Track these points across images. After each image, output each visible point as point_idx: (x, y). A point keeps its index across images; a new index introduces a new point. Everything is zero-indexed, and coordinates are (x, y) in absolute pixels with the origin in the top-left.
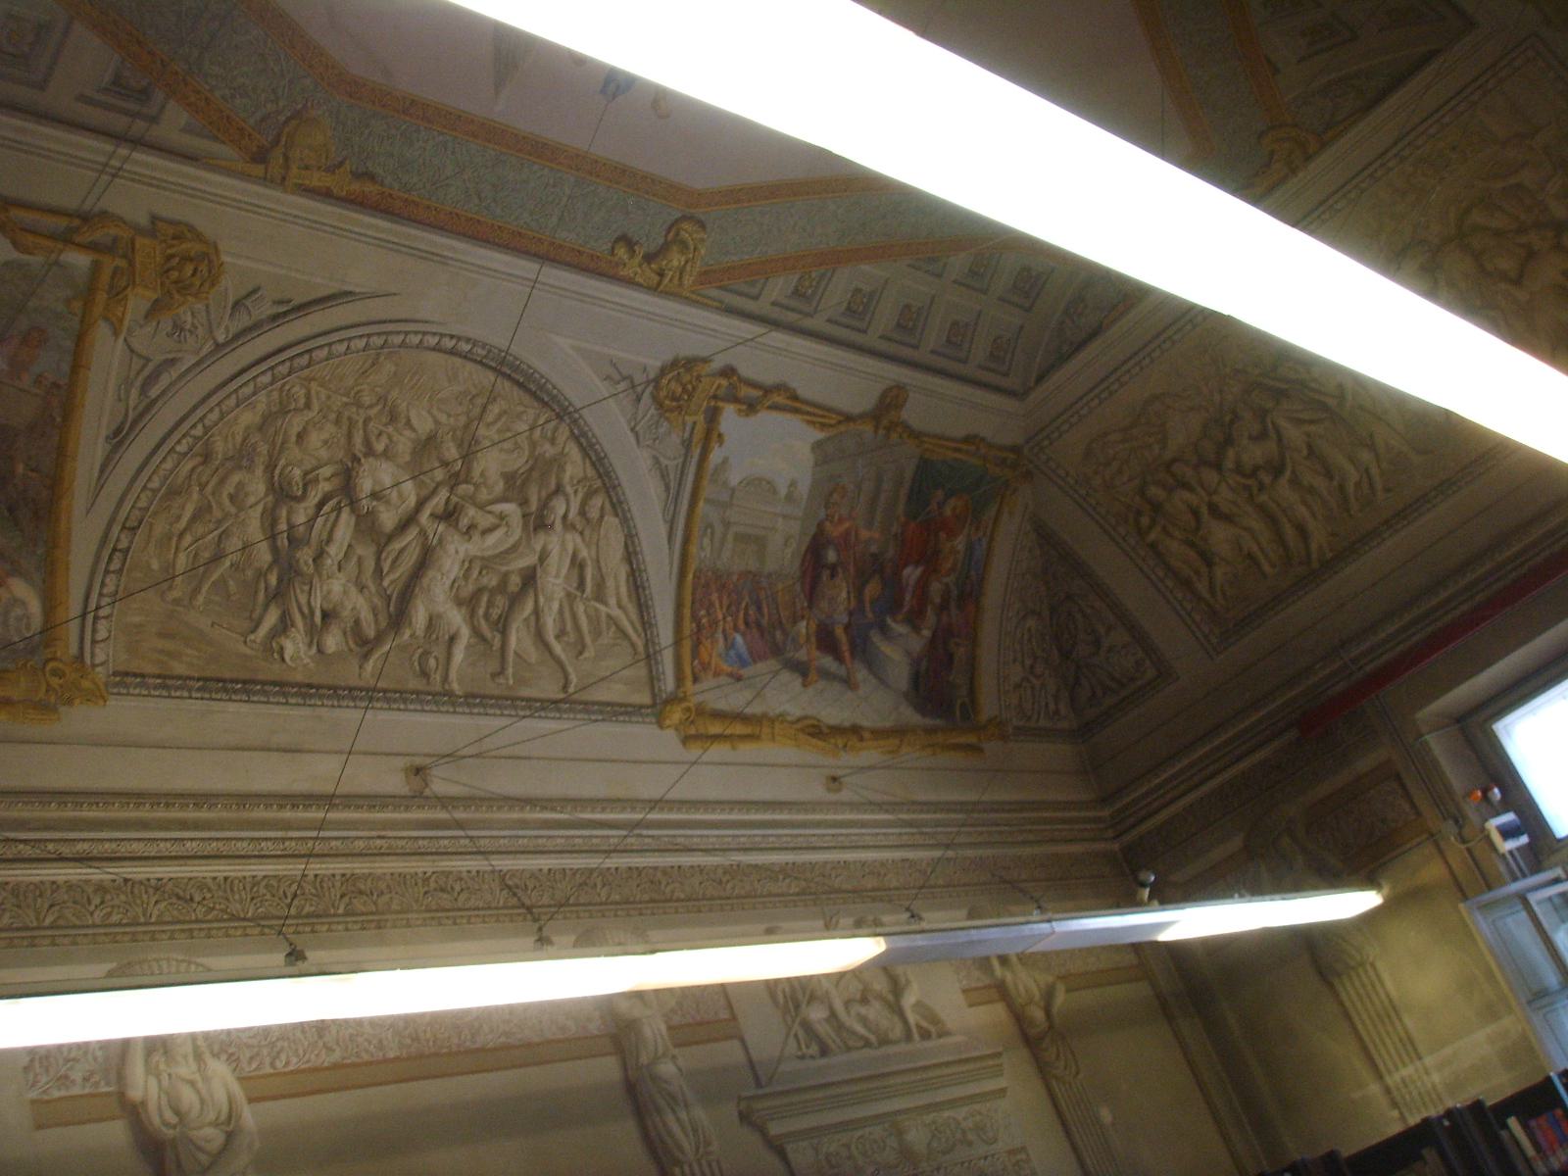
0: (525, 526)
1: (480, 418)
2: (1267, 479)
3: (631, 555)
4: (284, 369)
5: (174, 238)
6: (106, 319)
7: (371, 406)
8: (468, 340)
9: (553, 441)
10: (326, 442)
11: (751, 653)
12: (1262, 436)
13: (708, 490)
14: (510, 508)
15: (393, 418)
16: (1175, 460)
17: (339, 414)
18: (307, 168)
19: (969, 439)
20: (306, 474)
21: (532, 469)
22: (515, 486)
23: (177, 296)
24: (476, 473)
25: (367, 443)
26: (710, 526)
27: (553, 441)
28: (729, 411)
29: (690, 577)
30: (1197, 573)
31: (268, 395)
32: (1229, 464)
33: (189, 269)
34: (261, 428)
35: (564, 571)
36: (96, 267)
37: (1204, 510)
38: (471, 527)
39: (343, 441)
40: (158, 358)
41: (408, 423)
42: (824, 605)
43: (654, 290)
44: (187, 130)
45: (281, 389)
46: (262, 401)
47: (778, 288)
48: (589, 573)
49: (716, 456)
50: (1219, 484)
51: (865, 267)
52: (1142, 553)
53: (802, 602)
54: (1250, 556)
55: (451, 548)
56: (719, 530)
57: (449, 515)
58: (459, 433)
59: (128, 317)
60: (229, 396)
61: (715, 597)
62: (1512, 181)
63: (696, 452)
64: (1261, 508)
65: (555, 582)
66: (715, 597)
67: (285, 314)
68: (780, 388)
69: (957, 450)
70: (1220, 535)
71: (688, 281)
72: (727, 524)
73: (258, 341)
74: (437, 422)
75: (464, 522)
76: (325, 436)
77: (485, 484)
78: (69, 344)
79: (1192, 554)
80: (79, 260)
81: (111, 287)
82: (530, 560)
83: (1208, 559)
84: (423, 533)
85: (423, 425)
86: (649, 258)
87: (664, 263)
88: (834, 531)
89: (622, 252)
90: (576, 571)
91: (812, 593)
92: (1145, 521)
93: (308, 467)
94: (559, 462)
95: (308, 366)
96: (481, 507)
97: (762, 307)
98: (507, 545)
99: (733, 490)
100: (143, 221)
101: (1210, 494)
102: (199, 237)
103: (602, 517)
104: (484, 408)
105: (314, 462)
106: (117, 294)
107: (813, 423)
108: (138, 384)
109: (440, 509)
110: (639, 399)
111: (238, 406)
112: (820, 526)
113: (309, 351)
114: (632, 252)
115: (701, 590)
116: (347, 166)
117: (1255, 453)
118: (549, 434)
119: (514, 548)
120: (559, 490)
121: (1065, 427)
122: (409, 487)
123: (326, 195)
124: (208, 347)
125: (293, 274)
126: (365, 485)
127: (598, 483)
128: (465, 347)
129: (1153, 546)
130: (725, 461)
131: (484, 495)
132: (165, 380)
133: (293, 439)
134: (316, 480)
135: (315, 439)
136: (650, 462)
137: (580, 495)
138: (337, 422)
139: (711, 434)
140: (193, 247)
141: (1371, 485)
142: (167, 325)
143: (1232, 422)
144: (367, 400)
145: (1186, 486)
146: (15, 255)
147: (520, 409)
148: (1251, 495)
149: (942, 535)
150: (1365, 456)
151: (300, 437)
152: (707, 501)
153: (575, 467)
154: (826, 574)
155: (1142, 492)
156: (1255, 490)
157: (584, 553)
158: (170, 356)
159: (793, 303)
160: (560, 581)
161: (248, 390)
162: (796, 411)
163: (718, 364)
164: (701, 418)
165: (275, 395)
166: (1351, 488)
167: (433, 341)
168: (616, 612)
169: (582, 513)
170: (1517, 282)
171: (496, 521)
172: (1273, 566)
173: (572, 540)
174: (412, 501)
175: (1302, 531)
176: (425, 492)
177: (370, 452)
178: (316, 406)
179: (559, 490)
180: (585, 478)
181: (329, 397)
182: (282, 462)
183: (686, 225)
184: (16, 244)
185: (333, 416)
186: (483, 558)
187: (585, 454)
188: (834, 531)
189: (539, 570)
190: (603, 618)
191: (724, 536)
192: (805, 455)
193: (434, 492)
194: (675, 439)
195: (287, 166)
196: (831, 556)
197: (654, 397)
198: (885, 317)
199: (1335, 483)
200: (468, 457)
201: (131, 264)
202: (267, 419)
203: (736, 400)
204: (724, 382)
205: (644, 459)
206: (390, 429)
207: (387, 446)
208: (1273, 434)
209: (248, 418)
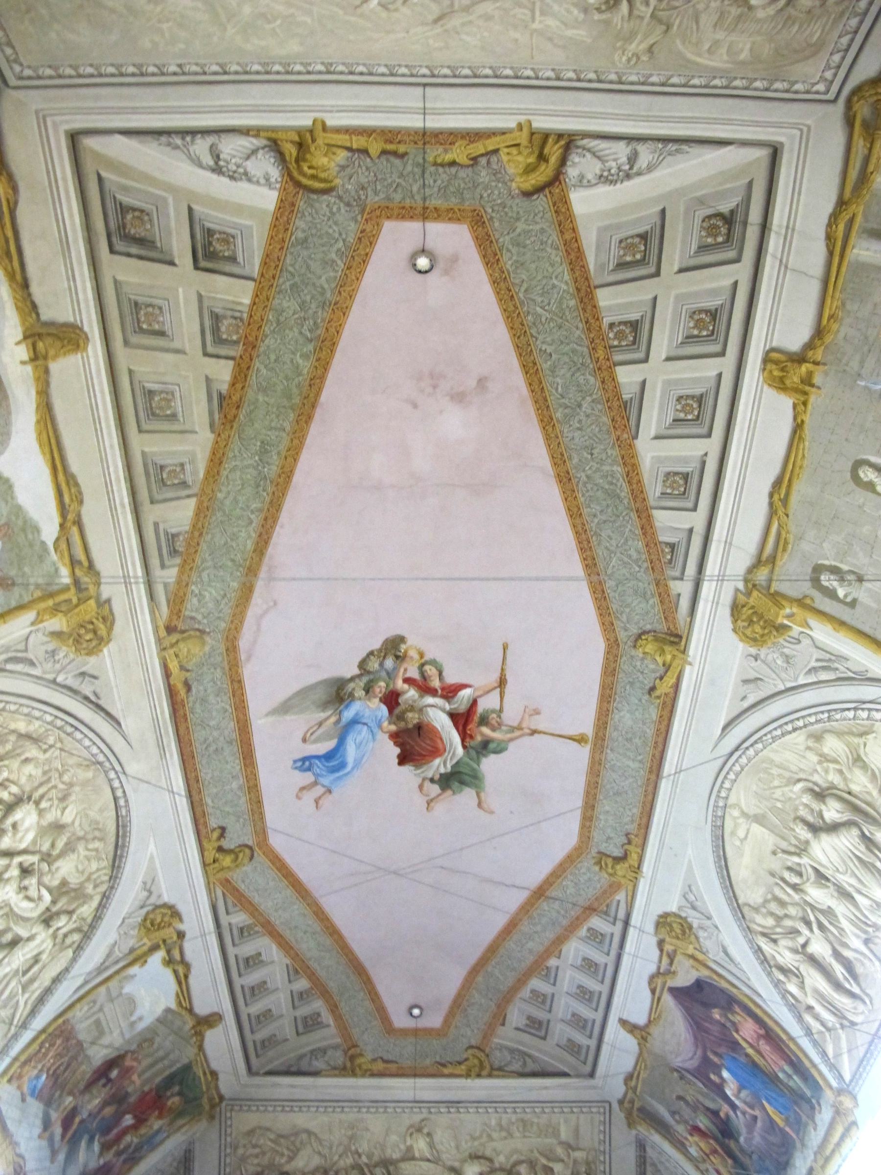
0: (43, 913)
1: (87, 841)
3: (57, 980)
4: (59, 723)
5: (103, 618)
6: (38, 614)
7: (63, 783)
8: (127, 801)
9: (96, 886)
10: (30, 775)
11: (41, 1090)
13: (113, 984)
14: (47, 897)
15: (63, 798)
17: (50, 770)
18: (177, 656)
19: (214, 1074)
20: (7, 780)
21: (75, 890)
22: (62, 890)
23: (71, 641)
24: (57, 864)
25: (42, 797)
26: (95, 1002)
27: (96, 886)
28: (161, 954)
29: (60, 1021)
31: (40, 727)
33: (88, 637)
34: (21, 736)
35: (29, 956)
36: (66, 589)
38: (26, 888)
39: (36, 784)
40: (30, 655)
41: (64, 809)
42: (87, 1097)
43: (205, 865)
44: (166, 585)
45: (47, 730)
46: (35, 727)
47: (240, 918)
48: (36, 969)
49: (135, 970)
51: (274, 947)
53: (81, 1086)
55: (8, 888)
56: (95, 1009)
57: (25, 871)
58: (73, 838)
59: (45, 624)
60: (28, 706)
61: (59, 1042)
62: (551, 1165)
63: (131, 958)
65: (20, 957)
66: (59, 1042)
67: (91, 702)
68: (187, 966)
69: (205, 1074)
71: (219, 875)
72: (101, 1009)
73: (67, 698)
74: (73, 822)
75: (26, 882)
76: (34, 773)
77: (53, 874)
78: (13, 604)
80: (65, 577)
81: (59, 604)
82: (23, 933)
84: (8, 867)
85: (67, 818)
86: (220, 849)
87: (221, 857)
88: (128, 1062)
89: (216, 835)
90: (32, 961)
91: (90, 1085)
93: (11, 777)
94: (87, 898)
95: (68, 734)
96: (40, 883)
97: (224, 919)
98: (26, 915)
99: (120, 994)
100: (104, 596)
102: (110, 629)
103: (70, 946)
104: (94, 839)
105: (16, 779)
106: (55, 610)
107: (177, 995)
108: (10, 655)
109: (26, 865)
110: (142, 907)
111: (26, 715)
112: (127, 1052)
113: (76, 729)
114: (219, 839)
115: (61, 1033)
116: (188, 674)
118: (98, 881)
119: (26, 920)
120: (70, 913)
122: (30, 836)
123: (167, 674)
124: (50, 677)
125: (115, 690)
126: (18, 815)
127: (85, 928)
128: (122, 802)
130: (133, 977)
131: (46, 879)
132: (19, 667)
133: (23, 757)
134: (6, 788)
135: (29, 769)
136: (112, 941)
137: (75, 926)
138: (45, 773)
139: (138, 958)
140: (102, 631)
142: (50, 647)
144: (66, 778)
146: (50, 544)
147: (104, 857)
149: (157, 1113)
151: (27, 760)
152: (108, 990)
153: (87, 910)
154: (103, 1081)
157: (44, 957)
158: (35, 661)
159: (235, 932)
160: (22, 959)
161: (37, 714)
162: (179, 983)
163: (181, 927)
164: (149, 944)
165: (42, 730)
167: (116, 784)
168: (22, 1003)
169: (65, 936)
171: (36, 897)
173: (49, 944)
174: (23, 846)
176: (31, 849)
177: (37, 803)
178: (48, 755)
179: (70, 913)
180: (84, 919)
181: (56, 758)
182: (6, 762)
183: (247, 851)
184: (57, 540)
185: (46, 768)
186: (11, 909)
187: (97, 909)
188: (128, 1062)
189: (20, 945)
190: (15, 1000)
191: (94, 1014)
192: (159, 1011)
193: (33, 853)
194: (131, 942)
195: (172, 646)
196: (114, 1074)
197: (148, 913)
198: (253, 978)
200: (62, 854)
201: (77, 606)
202: (28, 737)
203: (168, 952)
204: (175, 938)
205: (112, 937)
206: (56, 802)
207: (44, 810)
209: (21, 726)
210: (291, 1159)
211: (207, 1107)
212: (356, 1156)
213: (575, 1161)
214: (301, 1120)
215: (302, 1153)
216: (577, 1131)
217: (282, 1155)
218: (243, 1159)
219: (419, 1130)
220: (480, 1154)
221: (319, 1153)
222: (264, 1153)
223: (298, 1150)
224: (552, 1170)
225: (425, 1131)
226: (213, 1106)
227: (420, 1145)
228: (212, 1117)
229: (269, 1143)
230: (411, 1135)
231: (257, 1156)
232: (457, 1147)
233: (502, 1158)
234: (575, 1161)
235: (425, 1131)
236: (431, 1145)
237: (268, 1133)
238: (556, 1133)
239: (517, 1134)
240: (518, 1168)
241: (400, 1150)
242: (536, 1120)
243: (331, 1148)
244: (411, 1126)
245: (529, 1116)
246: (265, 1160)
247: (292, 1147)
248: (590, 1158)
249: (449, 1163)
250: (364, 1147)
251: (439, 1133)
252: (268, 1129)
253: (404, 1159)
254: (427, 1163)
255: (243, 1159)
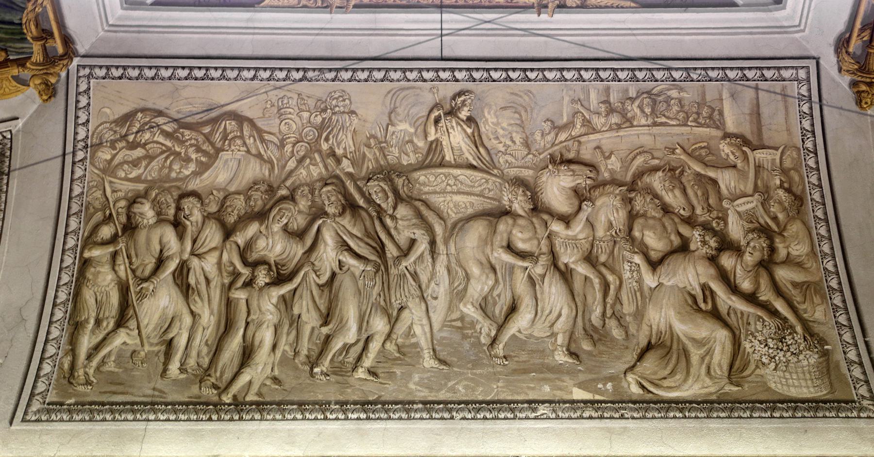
2: (262, 278)
12: (299, 235)
16: (194, 194)
30: (98, 322)
32: (240, 239)
37: (172, 266)
50: (215, 249)
52: (68, 261)
54: (170, 344)
62: (711, 174)
64: (229, 304)
70: (160, 302)
79: (115, 299)
83: (124, 315)
92: (106, 232)
101: (192, 254)
117: (274, 245)
121: (135, 73)
129: (85, 263)
141: (359, 358)
143: (283, 199)
145: (177, 225)
148: (231, 284)
150: (379, 325)
155: (133, 201)
156: (240, 283)
166: (337, 345)
170: (654, 265)
172: (182, 370)
175: (247, 355)
199: (325, 330)
208: (309, 242)
210: (203, 168)
211: (37, 56)
212: (330, 161)
213: (758, 168)
214: (222, 93)
215: (224, 156)
216: (756, 114)
217: (188, 160)
218: (109, 169)
219: (452, 113)
220: (571, 155)
221: (259, 156)
222: (150, 158)
223: (218, 151)
224: (715, 182)
225: (464, 114)
226: (50, 60)
227: (455, 139)
228: (49, 91)
229: (161, 139)
230: (437, 121)
231: (135, 163)
232: (527, 144)
233: (614, 163)
234: (758, 168)
235: (464, 114)
236: (477, 141)
237: (160, 120)
238: (715, 120)
239: (643, 121)
240: (647, 179)
241: (416, 150)
242: (674, 93)
243: (282, 145)
244: (437, 106)
245: (662, 86)
246: (153, 170)
247: (206, 147)
248: (788, 163)
249: (513, 172)
250: (345, 143)
251: (491, 118)
252: (160, 113)
253: (422, 166)
254: (469, 172)
255: (109, 169)
